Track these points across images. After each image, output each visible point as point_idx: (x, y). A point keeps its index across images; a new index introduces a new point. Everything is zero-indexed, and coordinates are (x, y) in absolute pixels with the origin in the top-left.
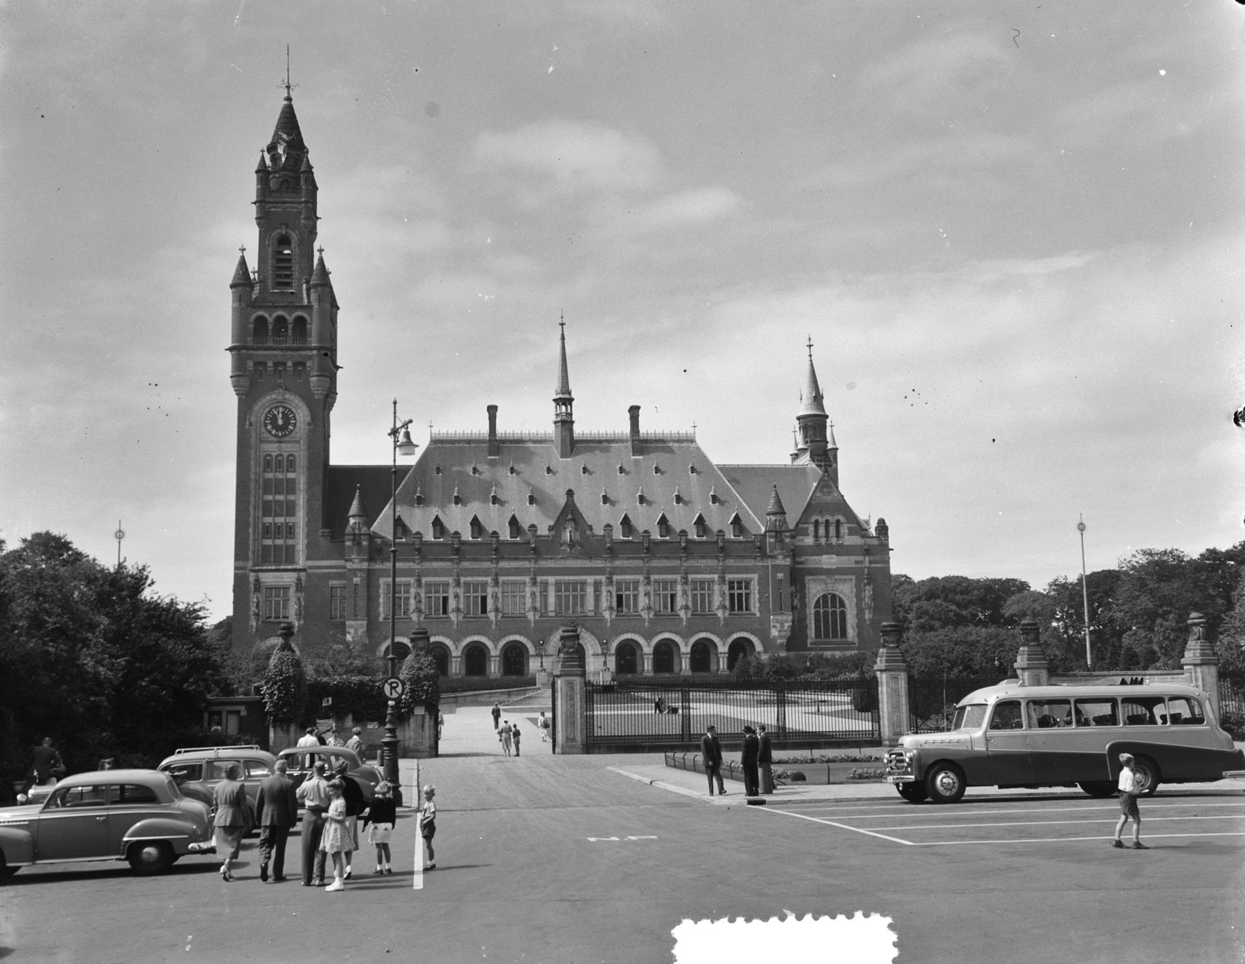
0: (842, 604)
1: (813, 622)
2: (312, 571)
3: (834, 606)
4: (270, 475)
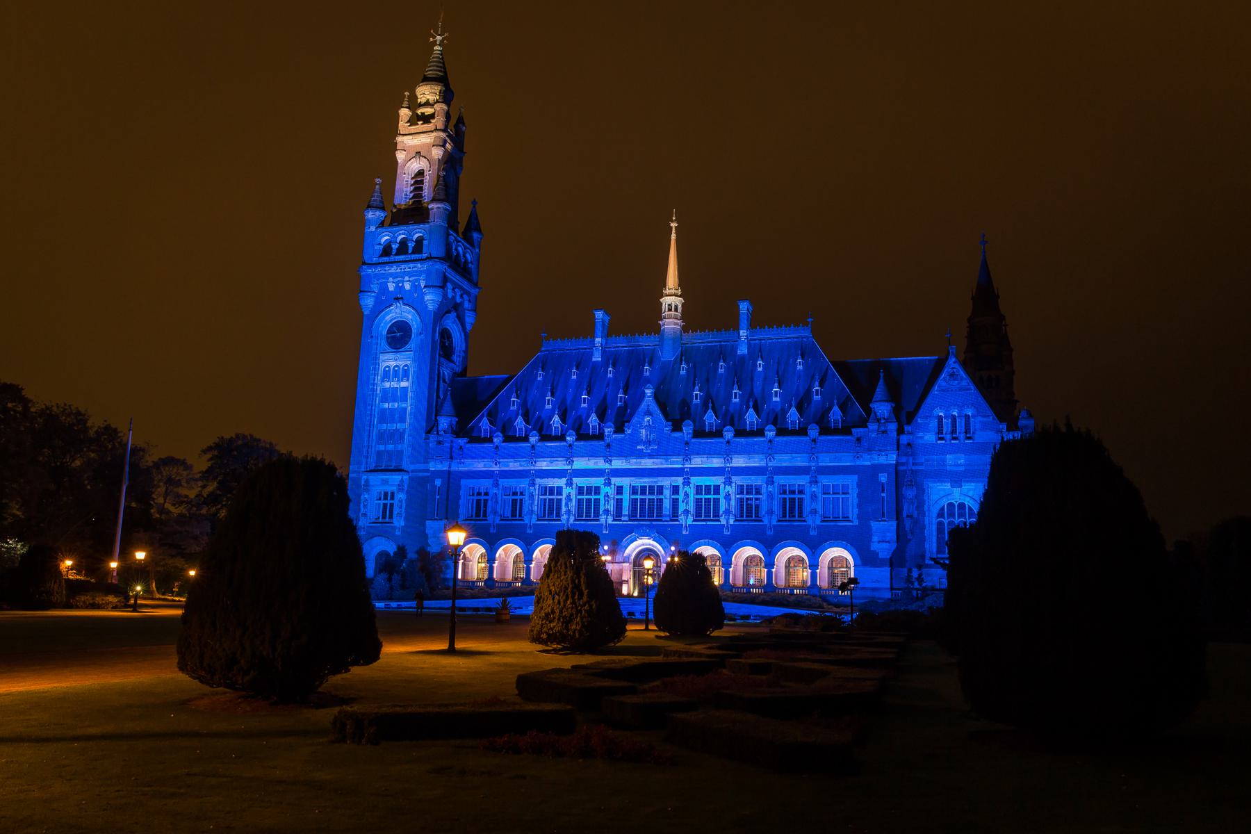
2: (414, 474)
4: (387, 385)
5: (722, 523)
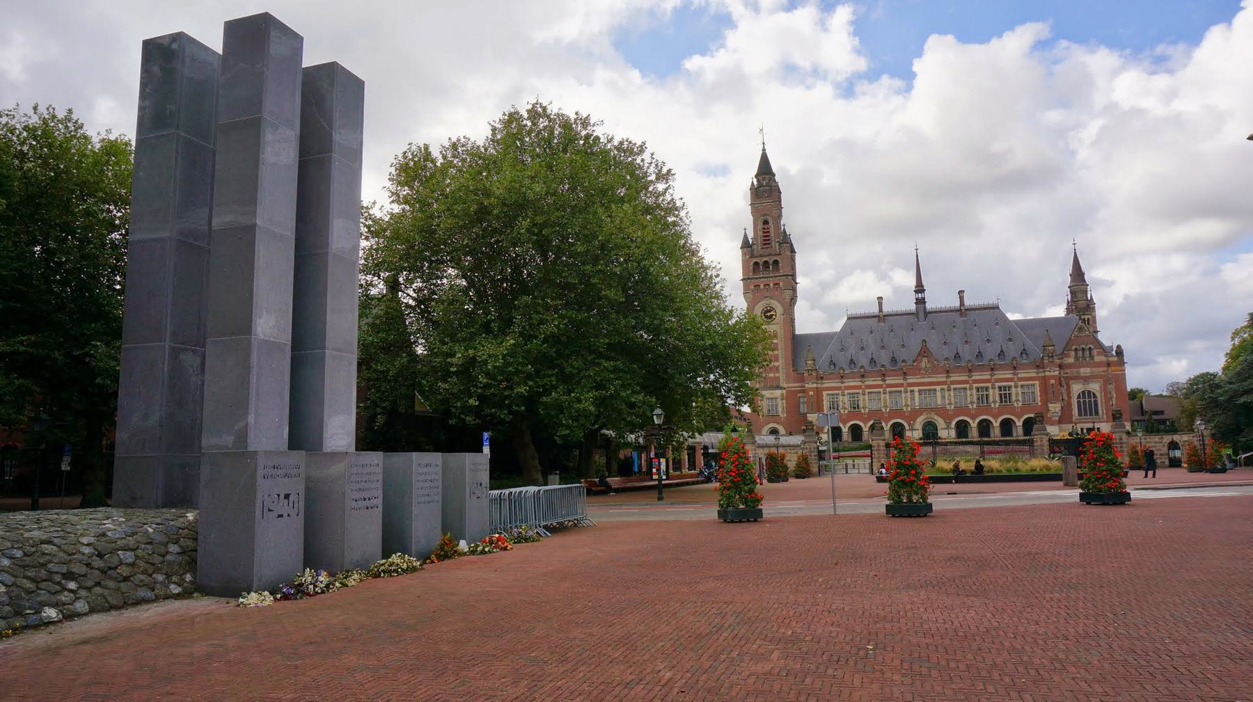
0: (1095, 396)
1: (1076, 407)
2: (789, 389)
3: (1090, 397)
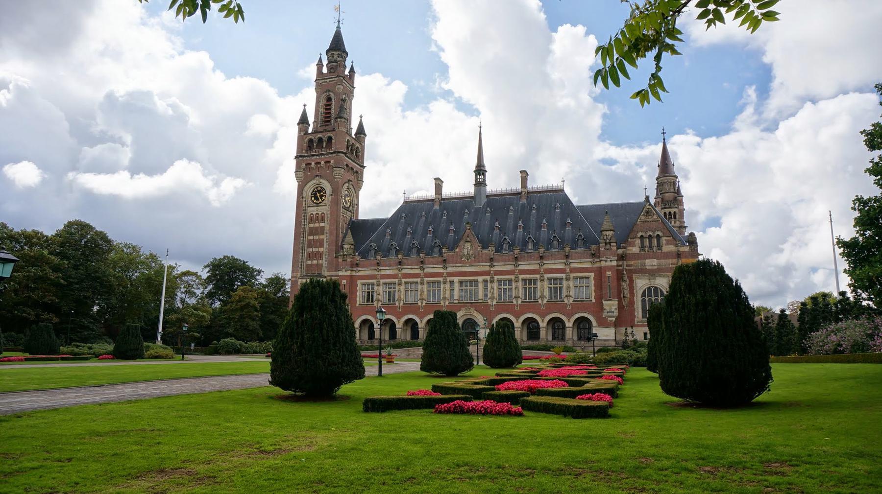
1: (640, 306)
3: (656, 295)
4: (312, 225)
5: (514, 303)
